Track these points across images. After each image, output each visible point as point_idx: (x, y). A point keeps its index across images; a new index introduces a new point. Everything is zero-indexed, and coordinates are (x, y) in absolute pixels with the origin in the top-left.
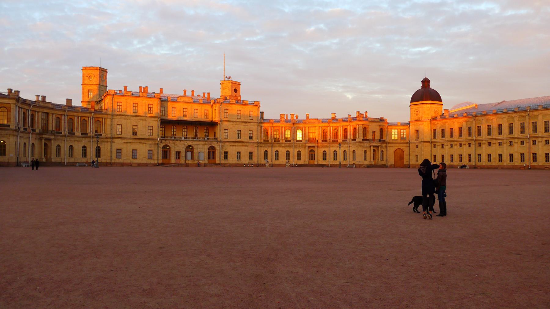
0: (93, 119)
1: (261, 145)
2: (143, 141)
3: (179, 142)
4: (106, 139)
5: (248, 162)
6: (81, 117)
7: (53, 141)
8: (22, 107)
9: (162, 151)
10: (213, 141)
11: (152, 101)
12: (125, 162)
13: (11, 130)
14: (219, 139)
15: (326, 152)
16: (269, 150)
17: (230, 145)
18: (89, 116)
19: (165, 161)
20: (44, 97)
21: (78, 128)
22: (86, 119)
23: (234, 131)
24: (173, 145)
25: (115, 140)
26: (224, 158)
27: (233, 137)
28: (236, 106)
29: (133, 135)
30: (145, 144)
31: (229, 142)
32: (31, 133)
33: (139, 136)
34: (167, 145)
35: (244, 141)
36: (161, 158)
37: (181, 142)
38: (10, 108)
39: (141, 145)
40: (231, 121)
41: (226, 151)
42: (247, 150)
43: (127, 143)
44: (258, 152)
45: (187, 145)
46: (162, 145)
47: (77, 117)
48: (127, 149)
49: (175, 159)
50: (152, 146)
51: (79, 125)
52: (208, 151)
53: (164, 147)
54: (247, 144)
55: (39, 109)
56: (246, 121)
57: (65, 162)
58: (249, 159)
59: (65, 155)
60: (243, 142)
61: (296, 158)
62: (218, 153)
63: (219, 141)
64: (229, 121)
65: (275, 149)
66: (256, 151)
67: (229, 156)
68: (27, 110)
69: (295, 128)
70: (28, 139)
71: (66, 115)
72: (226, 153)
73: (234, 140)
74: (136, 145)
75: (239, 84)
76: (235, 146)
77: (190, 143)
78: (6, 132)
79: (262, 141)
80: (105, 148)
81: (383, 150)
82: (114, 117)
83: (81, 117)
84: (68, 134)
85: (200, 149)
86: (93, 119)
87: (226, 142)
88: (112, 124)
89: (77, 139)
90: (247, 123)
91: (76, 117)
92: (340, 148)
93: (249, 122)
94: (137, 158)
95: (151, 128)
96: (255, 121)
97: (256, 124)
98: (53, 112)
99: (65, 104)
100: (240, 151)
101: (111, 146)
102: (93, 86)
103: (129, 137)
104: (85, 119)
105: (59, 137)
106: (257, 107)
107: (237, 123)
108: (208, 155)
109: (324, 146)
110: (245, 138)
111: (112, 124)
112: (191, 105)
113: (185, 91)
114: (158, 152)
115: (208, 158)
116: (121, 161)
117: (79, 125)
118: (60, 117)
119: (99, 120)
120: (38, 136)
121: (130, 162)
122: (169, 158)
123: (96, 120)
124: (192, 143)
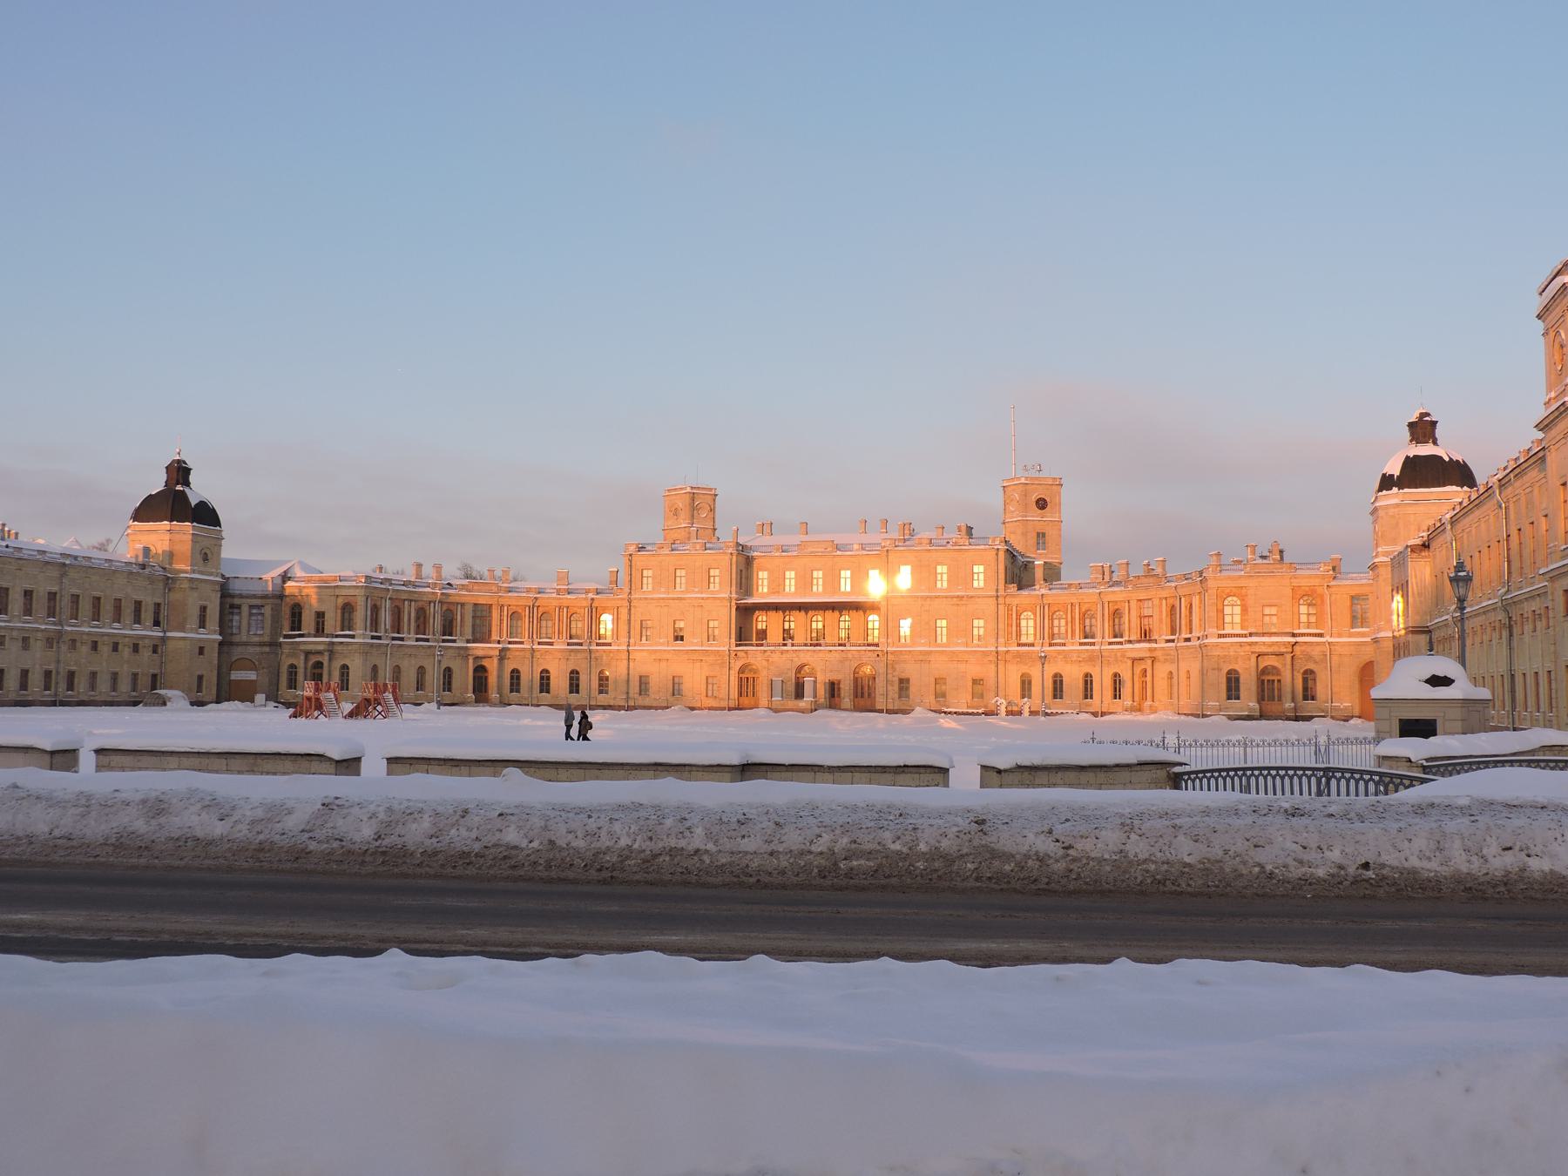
15: (1091, 676)
16: (1035, 673)
22: (578, 611)
24: (765, 663)
26: (897, 696)
30: (698, 664)
37: (784, 655)
41: (904, 676)
46: (737, 665)
53: (742, 670)
59: (531, 689)
61: (1109, 693)
65: (1050, 670)
67: (913, 689)
69: (1106, 605)
78: (350, 648)
81: (1311, 666)
85: (831, 671)
92: (1043, 664)
102: (679, 531)
106: (995, 553)
109: (1168, 657)
116: (647, 702)
118: (520, 611)
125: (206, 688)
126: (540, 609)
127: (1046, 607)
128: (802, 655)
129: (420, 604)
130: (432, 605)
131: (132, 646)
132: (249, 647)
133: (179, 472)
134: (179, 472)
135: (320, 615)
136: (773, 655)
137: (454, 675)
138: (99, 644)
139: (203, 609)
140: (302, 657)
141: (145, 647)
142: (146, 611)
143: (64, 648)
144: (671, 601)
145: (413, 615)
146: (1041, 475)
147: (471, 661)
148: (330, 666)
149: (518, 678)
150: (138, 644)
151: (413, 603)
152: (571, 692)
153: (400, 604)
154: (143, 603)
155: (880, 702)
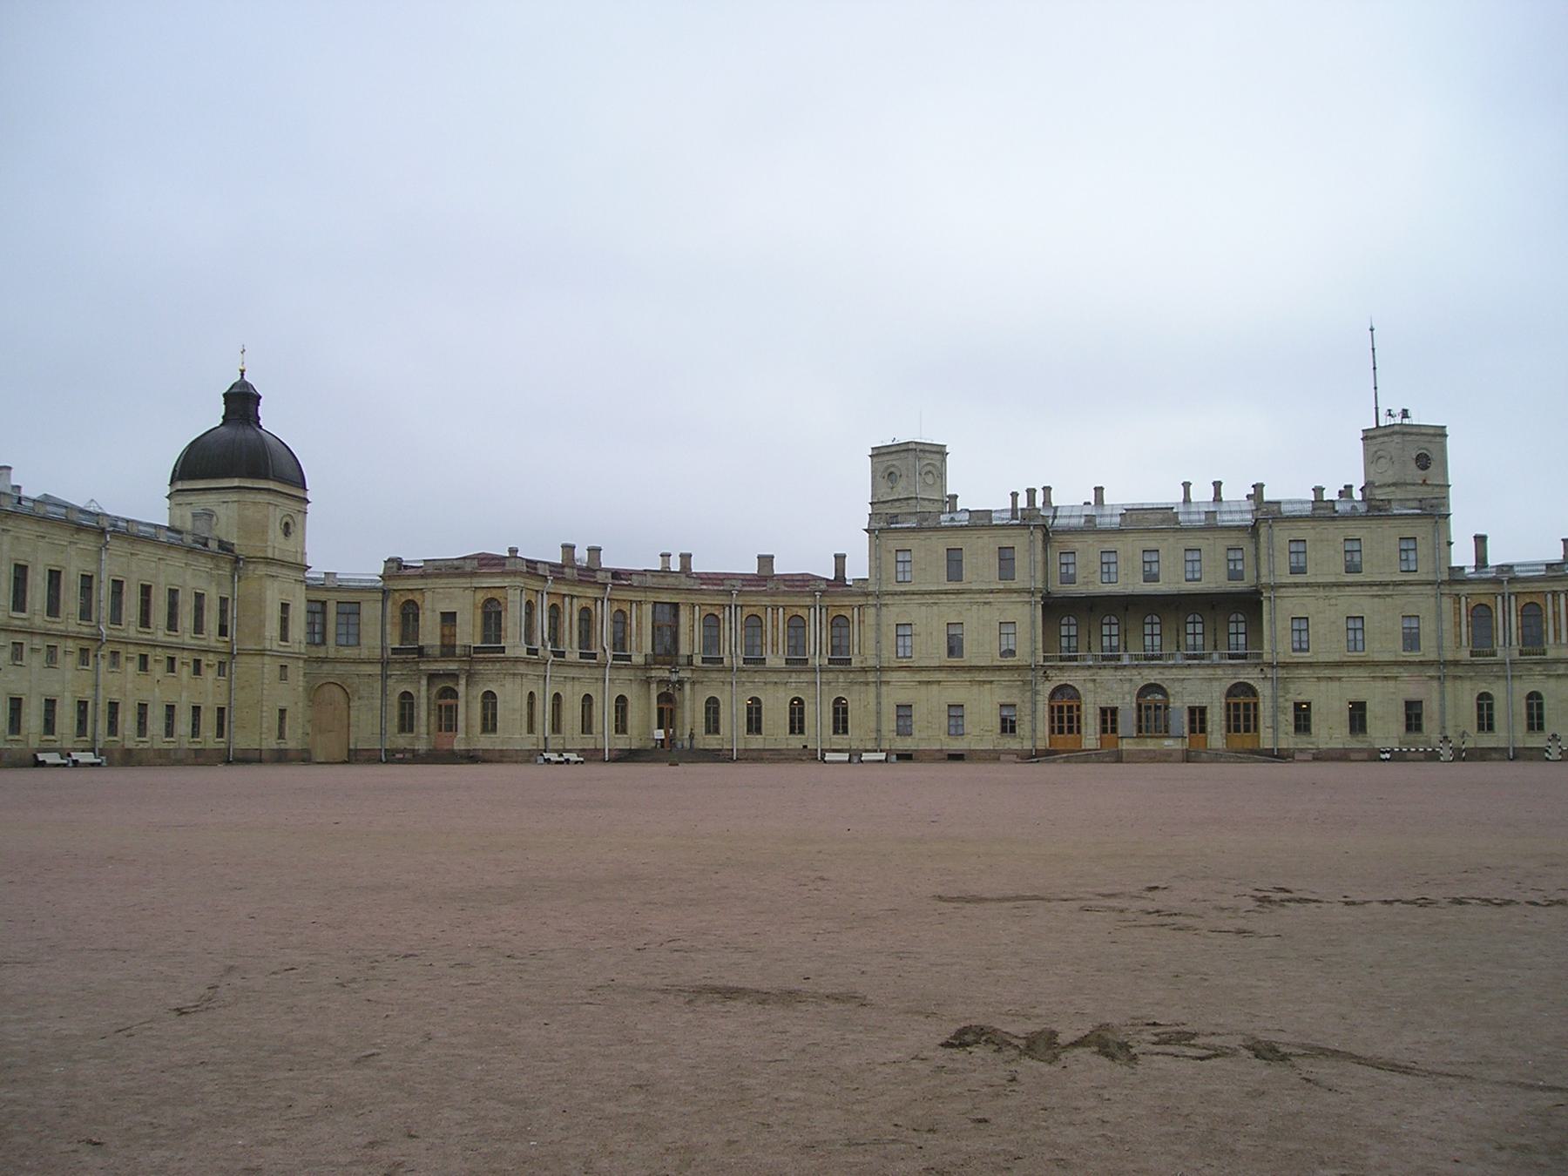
0: (824, 610)
1: (1459, 671)
2: (982, 677)
3: (1112, 672)
4: (863, 673)
5: (1400, 743)
7: (687, 687)
8: (575, 593)
9: (1052, 708)
10: (1243, 666)
11: (1009, 537)
12: (923, 746)
13: (507, 659)
14: (1267, 658)
16: (1498, 691)
17: (1318, 678)
18: (810, 603)
19: (1064, 741)
20: (686, 558)
21: (775, 644)
23: (1334, 623)
24: (1090, 685)
25: (886, 677)
26: (1292, 729)
27: (1327, 643)
28: (1336, 522)
29: (948, 657)
30: (988, 686)
31: (1310, 665)
32: (608, 666)
33: (971, 656)
34: (1066, 684)
35: (1377, 657)
36: (1047, 733)
37: (1119, 673)
38: (506, 599)
39: (975, 689)
40: (1318, 585)
41: (1300, 699)
42: (1394, 693)
43: (929, 682)
44: (1443, 698)
47: (772, 609)
48: (930, 704)
49: (1098, 736)
50: (1015, 691)
51: (781, 635)
52: (1228, 705)
54: (1395, 671)
55: (643, 594)
56: (1388, 578)
57: (732, 750)
58: (1404, 728)
60: (1376, 664)
62: (1265, 709)
63: (1271, 665)
64: (1307, 585)
66: (1435, 695)
67: (1314, 719)
68: (596, 600)
70: (541, 682)
71: (736, 606)
73: (1335, 658)
74: (957, 694)
75: (1440, 433)
76: (1339, 679)
77: (1153, 676)
79: (1465, 655)
80: (860, 704)
82: (887, 600)
83: (782, 606)
84: (742, 662)
85: (1191, 695)
86: (824, 610)
87: (1298, 665)
88: (878, 625)
89: (774, 678)
90: (1391, 588)
91: (769, 609)
93: (1396, 584)
94: (963, 735)
95: (1359, 625)
96: (1424, 577)
97: (1429, 587)
98: (694, 599)
99: (756, 572)
101: (878, 696)
102: (897, 504)
103: (936, 663)
104: (799, 614)
105: (714, 675)
107: (1347, 589)
108: (1224, 718)
110: (1384, 644)
111: (878, 625)
112: (1171, 539)
113: (1186, 485)
114: (1034, 712)
115: (1229, 730)
117: (781, 635)
119: (843, 613)
120: (639, 673)
121: (939, 748)
122: (1079, 732)
123: (834, 615)
125: (290, 728)
127: (1513, 598)
128: (1146, 672)
129: (584, 603)
130: (599, 603)
131: (192, 664)
132: (338, 665)
133: (242, 402)
134: (242, 402)
135: (449, 618)
137: (629, 708)
138: (150, 659)
139: (285, 607)
140: (424, 682)
141: (208, 665)
142: (209, 611)
143: (104, 665)
144: (941, 596)
145: (576, 617)
146: (1406, 421)
147: (654, 686)
148: (467, 695)
149: (716, 711)
150: (200, 660)
151: (575, 600)
152: (792, 731)
153: (557, 601)
154: (206, 598)
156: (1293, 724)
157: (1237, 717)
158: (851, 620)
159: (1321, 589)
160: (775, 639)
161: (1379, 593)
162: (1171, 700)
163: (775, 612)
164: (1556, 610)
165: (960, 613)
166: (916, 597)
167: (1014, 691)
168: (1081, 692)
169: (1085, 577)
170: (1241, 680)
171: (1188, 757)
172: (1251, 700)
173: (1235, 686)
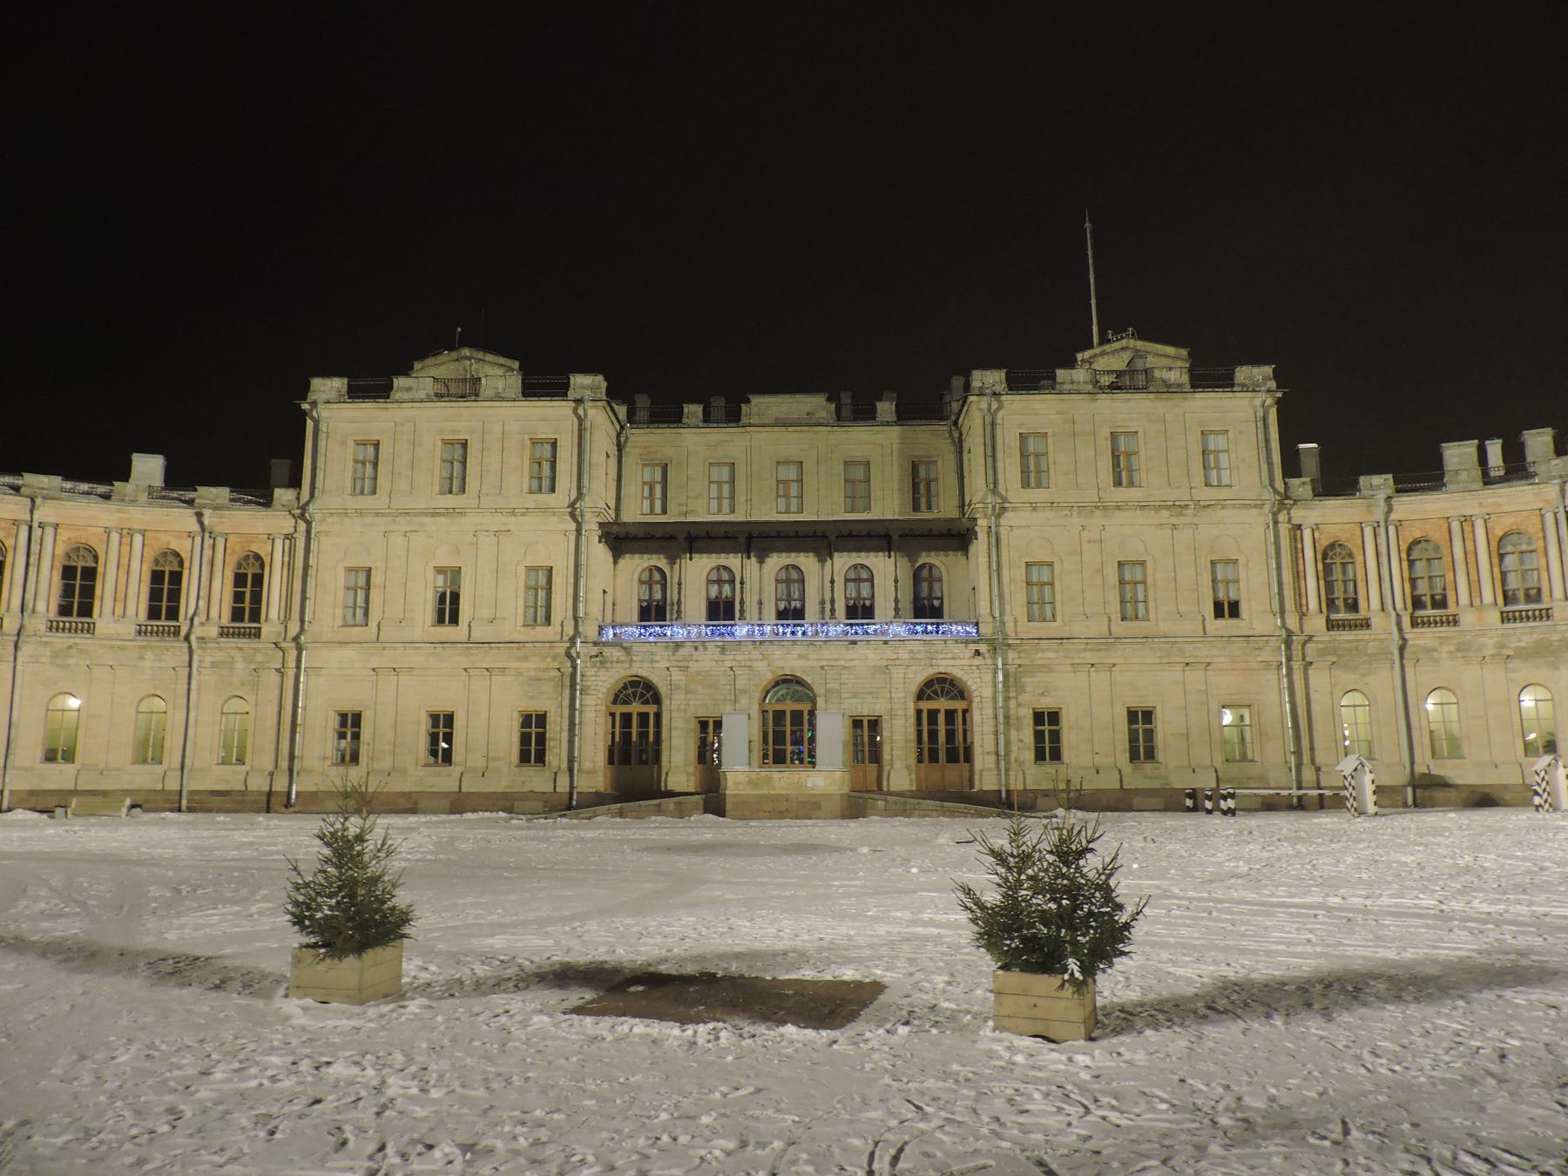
6: (143, 533)
24: (677, 676)
26: (1030, 755)
41: (1046, 703)
45: (770, 676)
50: (548, 688)
52: (919, 713)
67: (1068, 739)
72: (1047, 723)
77: (791, 661)
83: (143, 533)
85: (855, 695)
90: (1190, 511)
91: (115, 537)
97: (1254, 511)
100: (1148, 703)
115: (920, 761)
124: (802, 663)
126: (64, 535)
136: (700, 655)
144: (428, 519)
155: (986, 777)
156: (1033, 747)
157: (933, 734)
158: (267, 562)
159: (1075, 511)
160: (121, 589)
161: (1174, 520)
162: (820, 702)
163: (126, 540)
164: (1470, 547)
165: (457, 551)
166: (379, 520)
167: (544, 688)
168: (663, 690)
169: (680, 505)
170: (942, 670)
171: (854, 808)
172: (959, 705)
173: (929, 683)
